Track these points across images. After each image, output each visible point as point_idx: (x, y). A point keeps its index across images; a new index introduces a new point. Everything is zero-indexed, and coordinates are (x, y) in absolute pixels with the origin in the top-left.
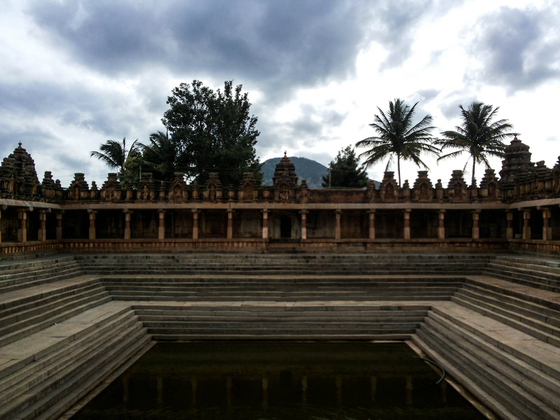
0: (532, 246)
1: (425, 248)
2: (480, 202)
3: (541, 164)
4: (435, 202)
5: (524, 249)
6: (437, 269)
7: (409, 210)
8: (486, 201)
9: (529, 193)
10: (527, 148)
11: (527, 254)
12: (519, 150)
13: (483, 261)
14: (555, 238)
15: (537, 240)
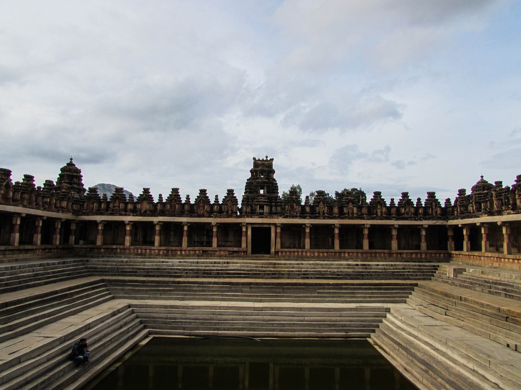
0: (110, 250)
1: (29, 255)
2: (63, 212)
3: (48, 183)
4: (38, 209)
5: (100, 253)
6: (68, 275)
7: (24, 215)
8: (66, 211)
9: (107, 210)
10: (79, 171)
11: (109, 257)
12: (77, 173)
13: (82, 265)
14: (132, 244)
15: (118, 246)
